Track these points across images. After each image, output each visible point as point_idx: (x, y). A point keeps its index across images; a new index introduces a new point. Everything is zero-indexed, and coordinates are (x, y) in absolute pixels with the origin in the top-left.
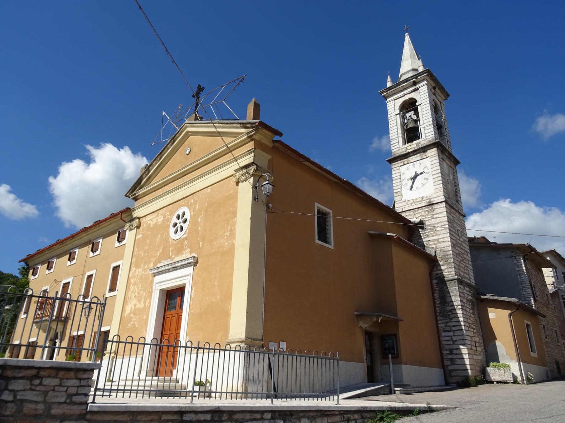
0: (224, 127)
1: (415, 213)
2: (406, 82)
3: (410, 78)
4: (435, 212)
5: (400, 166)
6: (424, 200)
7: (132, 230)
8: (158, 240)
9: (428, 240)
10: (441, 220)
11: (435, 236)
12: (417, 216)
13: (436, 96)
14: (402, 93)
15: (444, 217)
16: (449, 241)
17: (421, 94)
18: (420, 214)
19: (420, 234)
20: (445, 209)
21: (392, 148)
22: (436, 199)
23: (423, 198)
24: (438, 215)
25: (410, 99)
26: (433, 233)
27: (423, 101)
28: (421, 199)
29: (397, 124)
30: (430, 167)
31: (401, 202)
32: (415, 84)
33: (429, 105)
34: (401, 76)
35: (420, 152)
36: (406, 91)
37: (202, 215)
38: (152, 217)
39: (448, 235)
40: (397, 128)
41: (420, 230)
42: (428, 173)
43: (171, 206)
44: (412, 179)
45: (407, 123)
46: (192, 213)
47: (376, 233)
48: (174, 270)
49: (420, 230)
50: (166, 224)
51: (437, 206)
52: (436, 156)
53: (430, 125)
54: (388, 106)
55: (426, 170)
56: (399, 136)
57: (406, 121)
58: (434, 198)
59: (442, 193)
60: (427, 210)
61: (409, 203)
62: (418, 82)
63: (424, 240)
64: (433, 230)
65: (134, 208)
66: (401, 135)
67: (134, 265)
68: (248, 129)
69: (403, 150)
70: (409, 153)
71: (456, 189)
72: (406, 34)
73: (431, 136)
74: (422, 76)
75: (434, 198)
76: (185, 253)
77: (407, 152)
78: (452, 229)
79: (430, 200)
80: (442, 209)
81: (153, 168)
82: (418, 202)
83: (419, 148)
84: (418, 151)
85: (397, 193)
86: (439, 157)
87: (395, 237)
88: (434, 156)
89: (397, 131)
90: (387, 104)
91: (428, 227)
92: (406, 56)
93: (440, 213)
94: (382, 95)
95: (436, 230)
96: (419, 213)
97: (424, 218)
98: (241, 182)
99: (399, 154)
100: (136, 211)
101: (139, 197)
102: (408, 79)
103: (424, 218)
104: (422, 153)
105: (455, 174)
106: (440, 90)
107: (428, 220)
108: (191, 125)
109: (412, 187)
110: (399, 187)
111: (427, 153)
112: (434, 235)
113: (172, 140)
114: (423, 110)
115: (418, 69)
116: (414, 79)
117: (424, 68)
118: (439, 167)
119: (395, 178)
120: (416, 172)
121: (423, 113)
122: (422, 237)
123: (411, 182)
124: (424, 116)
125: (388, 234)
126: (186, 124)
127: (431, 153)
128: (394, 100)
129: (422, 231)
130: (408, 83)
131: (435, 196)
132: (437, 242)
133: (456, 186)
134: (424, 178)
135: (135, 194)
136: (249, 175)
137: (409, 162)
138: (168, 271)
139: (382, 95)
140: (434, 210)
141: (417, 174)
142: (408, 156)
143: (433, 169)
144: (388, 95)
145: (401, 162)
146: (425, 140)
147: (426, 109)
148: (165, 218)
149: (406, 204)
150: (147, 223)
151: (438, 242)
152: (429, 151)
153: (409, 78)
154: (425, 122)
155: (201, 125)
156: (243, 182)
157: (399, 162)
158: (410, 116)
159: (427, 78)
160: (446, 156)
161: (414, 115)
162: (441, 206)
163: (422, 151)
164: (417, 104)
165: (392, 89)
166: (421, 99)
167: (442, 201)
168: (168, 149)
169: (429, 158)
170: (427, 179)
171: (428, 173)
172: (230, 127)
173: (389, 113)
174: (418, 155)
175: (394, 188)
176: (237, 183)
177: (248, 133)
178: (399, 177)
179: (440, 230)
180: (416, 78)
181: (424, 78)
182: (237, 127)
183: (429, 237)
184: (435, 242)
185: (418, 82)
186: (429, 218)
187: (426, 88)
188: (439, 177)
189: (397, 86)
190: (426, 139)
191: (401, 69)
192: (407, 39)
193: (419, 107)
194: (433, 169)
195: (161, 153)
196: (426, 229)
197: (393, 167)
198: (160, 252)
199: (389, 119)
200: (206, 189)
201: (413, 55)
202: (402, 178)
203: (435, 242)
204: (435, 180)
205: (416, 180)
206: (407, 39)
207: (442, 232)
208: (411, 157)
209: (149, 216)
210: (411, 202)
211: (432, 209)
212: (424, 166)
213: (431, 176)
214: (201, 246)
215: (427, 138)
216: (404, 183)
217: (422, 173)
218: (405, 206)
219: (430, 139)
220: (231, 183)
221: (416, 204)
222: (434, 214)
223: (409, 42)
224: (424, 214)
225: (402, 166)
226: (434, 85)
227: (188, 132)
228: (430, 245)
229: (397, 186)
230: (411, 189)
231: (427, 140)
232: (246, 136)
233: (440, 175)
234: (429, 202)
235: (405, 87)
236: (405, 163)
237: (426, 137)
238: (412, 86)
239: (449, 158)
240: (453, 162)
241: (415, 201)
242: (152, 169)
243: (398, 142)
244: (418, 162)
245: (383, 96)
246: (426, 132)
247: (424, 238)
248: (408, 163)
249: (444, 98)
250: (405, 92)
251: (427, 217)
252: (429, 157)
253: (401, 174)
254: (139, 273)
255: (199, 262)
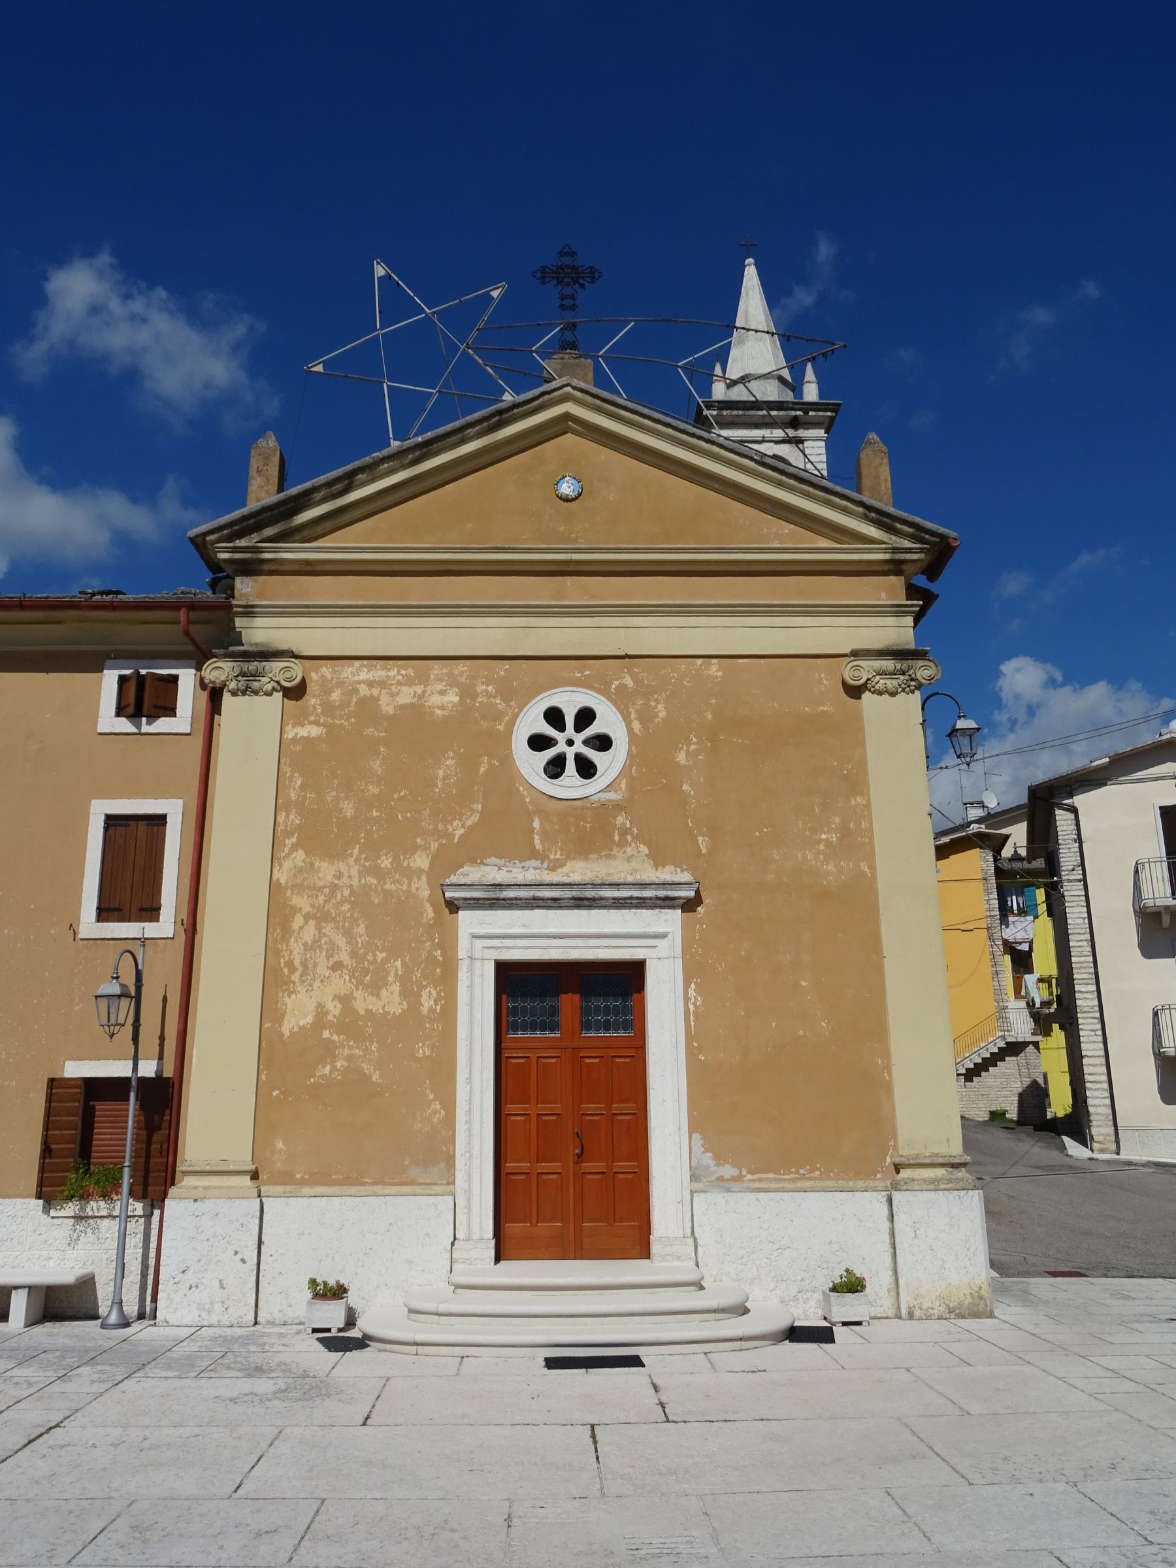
0: (779, 484)
2: (778, 410)
3: (790, 405)
7: (256, 693)
8: (441, 773)
32: (795, 423)
36: (769, 431)
37: (693, 747)
38: (384, 673)
43: (507, 665)
46: (637, 726)
48: (578, 907)
50: (485, 725)
65: (253, 606)
67: (294, 840)
68: (894, 538)
72: (750, 260)
76: (620, 854)
81: (373, 480)
98: (873, 693)
100: (259, 622)
101: (266, 567)
102: (785, 404)
108: (598, 402)
113: (492, 415)
116: (798, 413)
117: (821, 395)
126: (568, 389)
130: (782, 413)
135: (258, 550)
136: (913, 683)
138: (541, 903)
148: (475, 701)
150: (356, 691)
155: (647, 422)
156: (880, 693)
168: (464, 441)
172: (808, 496)
176: (854, 692)
177: (895, 550)
180: (806, 413)
181: (821, 420)
182: (845, 510)
192: (751, 274)
195: (428, 443)
198: (469, 823)
200: (699, 661)
206: (751, 274)
209: (358, 663)
214: (704, 850)
220: (820, 680)
227: (567, 416)
232: (887, 556)
242: (364, 484)
254: (344, 880)
255: (707, 901)
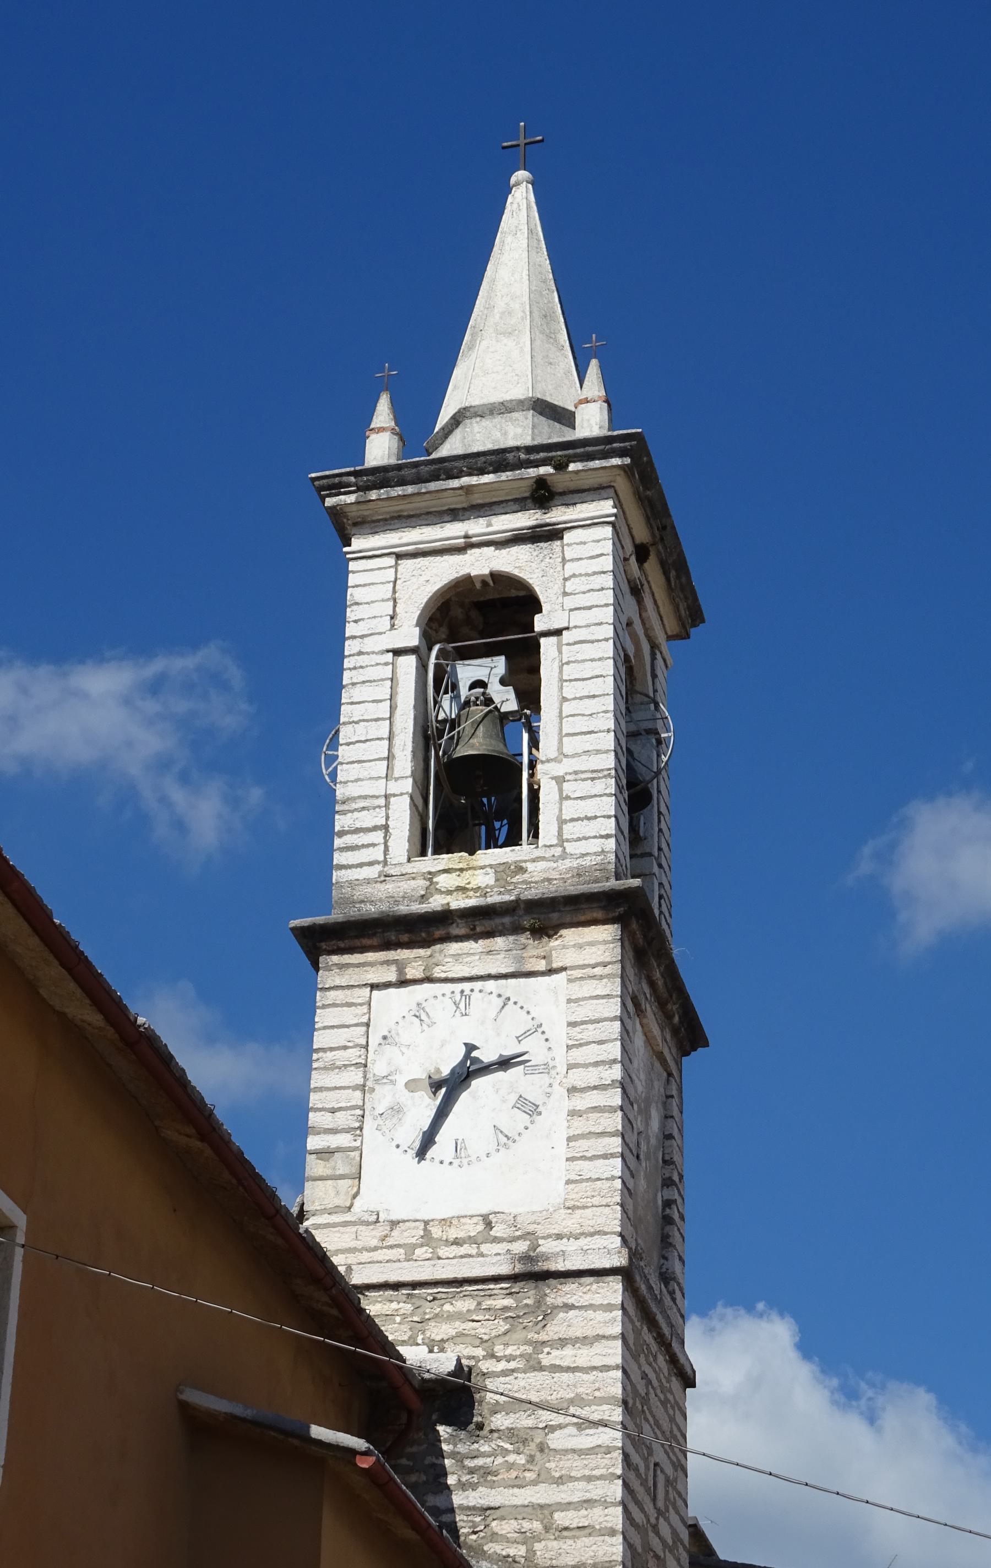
1: (430, 1310)
2: (494, 472)
3: (523, 456)
4: (555, 1329)
5: (374, 987)
6: (496, 1240)
9: (485, 1502)
10: (585, 1384)
11: (535, 1483)
12: (439, 1331)
13: (640, 602)
14: (454, 531)
15: (606, 1368)
16: (612, 1533)
17: (570, 568)
18: (460, 1326)
19: (441, 1454)
20: (614, 1324)
21: (338, 858)
22: (570, 1246)
23: (489, 1225)
24: (568, 1351)
25: (498, 578)
26: (521, 1460)
27: (578, 618)
28: (475, 1228)
29: (393, 709)
30: (560, 1034)
31: (346, 1224)
33: (608, 649)
34: (456, 421)
35: (516, 930)
36: (482, 521)
39: (616, 1491)
40: (390, 739)
41: (443, 1430)
42: (547, 1068)
44: (436, 1086)
45: (454, 723)
47: (238, 1410)
49: (443, 1430)
51: (572, 1292)
52: (608, 976)
53: (595, 775)
54: (352, 580)
55: (535, 1049)
56: (393, 787)
57: (448, 709)
58: (559, 1237)
59: (612, 1219)
60: (505, 1309)
61: (397, 1236)
62: (563, 494)
63: (458, 1499)
64: (525, 1442)
66: (408, 785)
69: (407, 886)
70: (444, 917)
71: (668, 1203)
72: (522, 175)
73: (594, 846)
74: (597, 464)
75: (559, 1237)
77: (436, 903)
78: (636, 1458)
79: (534, 1247)
80: (600, 1316)
82: (457, 1242)
83: (518, 901)
84: (507, 920)
85: (325, 1154)
86: (623, 985)
87: (365, 1463)
88: (598, 971)
89: (390, 758)
90: (352, 566)
91: (500, 1421)
92: (500, 304)
93: (586, 1341)
94: (330, 502)
95: (542, 1448)
96: (451, 1317)
97: (480, 1352)
99: (384, 907)
102: (510, 456)
103: (480, 1352)
104: (524, 939)
105: (675, 1112)
106: (666, 573)
107: (505, 1373)
109: (428, 1140)
110: (343, 1119)
111: (554, 943)
112: (530, 1476)
114: (569, 672)
115: (573, 414)
116: (548, 470)
117: (612, 424)
118: (615, 1050)
119: (330, 1055)
120: (470, 1048)
121: (569, 691)
122: (451, 1480)
123: (426, 1107)
124: (568, 708)
125: (318, 1432)
127: (580, 947)
128: (399, 556)
129: (453, 1440)
130: (504, 476)
131: (570, 1223)
132: (537, 1526)
133: (668, 1183)
134: (513, 1098)
137: (438, 973)
139: (330, 502)
140: (546, 1314)
141: (476, 1060)
142: (438, 933)
143: (579, 1055)
144: (365, 511)
145: (387, 963)
146: (554, 859)
147: (588, 670)
149: (374, 1242)
151: (547, 1529)
152: (569, 935)
153: (518, 449)
154: (570, 745)
157: (370, 956)
158: (479, 684)
159: (622, 484)
160: (652, 984)
161: (503, 682)
162: (598, 1300)
163: (526, 923)
164: (540, 623)
165: (402, 483)
166: (570, 602)
167: (607, 1264)
169: (561, 978)
170: (533, 1110)
171: (547, 1068)
173: (350, 630)
174: (500, 942)
175: (314, 1118)
178: (353, 1055)
179: (566, 1451)
180: (560, 467)
181: (603, 479)
183: (492, 1485)
184: (526, 1525)
185: (563, 494)
186: (509, 1359)
187: (608, 547)
188: (612, 1110)
189: (435, 477)
190: (564, 855)
191: (457, 373)
193: (547, 644)
194: (579, 1055)
196: (480, 1427)
197: (326, 978)
199: (347, 663)
201: (547, 316)
202: (378, 1067)
203: (526, 1525)
204: (580, 1126)
205: (465, 1098)
207: (577, 1466)
208: (454, 947)
210: (411, 1235)
211: (539, 1303)
212: (525, 1023)
213: (559, 1092)
215: (570, 848)
216: (382, 1099)
217: (504, 1063)
218: (365, 1256)
219: (587, 862)
221: (444, 1251)
222: (543, 1337)
223: (531, 231)
224: (483, 1330)
225: (387, 985)
226: (642, 535)
228: (494, 1537)
229: (333, 1111)
230: (421, 1153)
231: (568, 863)
233: (616, 1098)
234: (526, 1258)
235: (477, 499)
236: (411, 973)
237: (561, 841)
238: (520, 504)
239: (662, 1004)
240: (675, 1032)
241: (436, 1232)
243: (386, 828)
244: (491, 985)
245: (336, 514)
246: (571, 809)
247: (463, 1486)
248: (429, 980)
249: (672, 626)
250: (476, 527)
251: (499, 1350)
252: (563, 969)
253: (374, 1040)
